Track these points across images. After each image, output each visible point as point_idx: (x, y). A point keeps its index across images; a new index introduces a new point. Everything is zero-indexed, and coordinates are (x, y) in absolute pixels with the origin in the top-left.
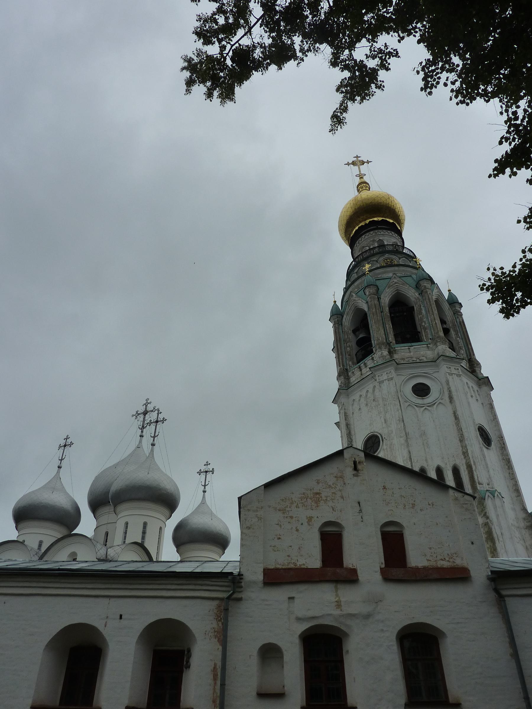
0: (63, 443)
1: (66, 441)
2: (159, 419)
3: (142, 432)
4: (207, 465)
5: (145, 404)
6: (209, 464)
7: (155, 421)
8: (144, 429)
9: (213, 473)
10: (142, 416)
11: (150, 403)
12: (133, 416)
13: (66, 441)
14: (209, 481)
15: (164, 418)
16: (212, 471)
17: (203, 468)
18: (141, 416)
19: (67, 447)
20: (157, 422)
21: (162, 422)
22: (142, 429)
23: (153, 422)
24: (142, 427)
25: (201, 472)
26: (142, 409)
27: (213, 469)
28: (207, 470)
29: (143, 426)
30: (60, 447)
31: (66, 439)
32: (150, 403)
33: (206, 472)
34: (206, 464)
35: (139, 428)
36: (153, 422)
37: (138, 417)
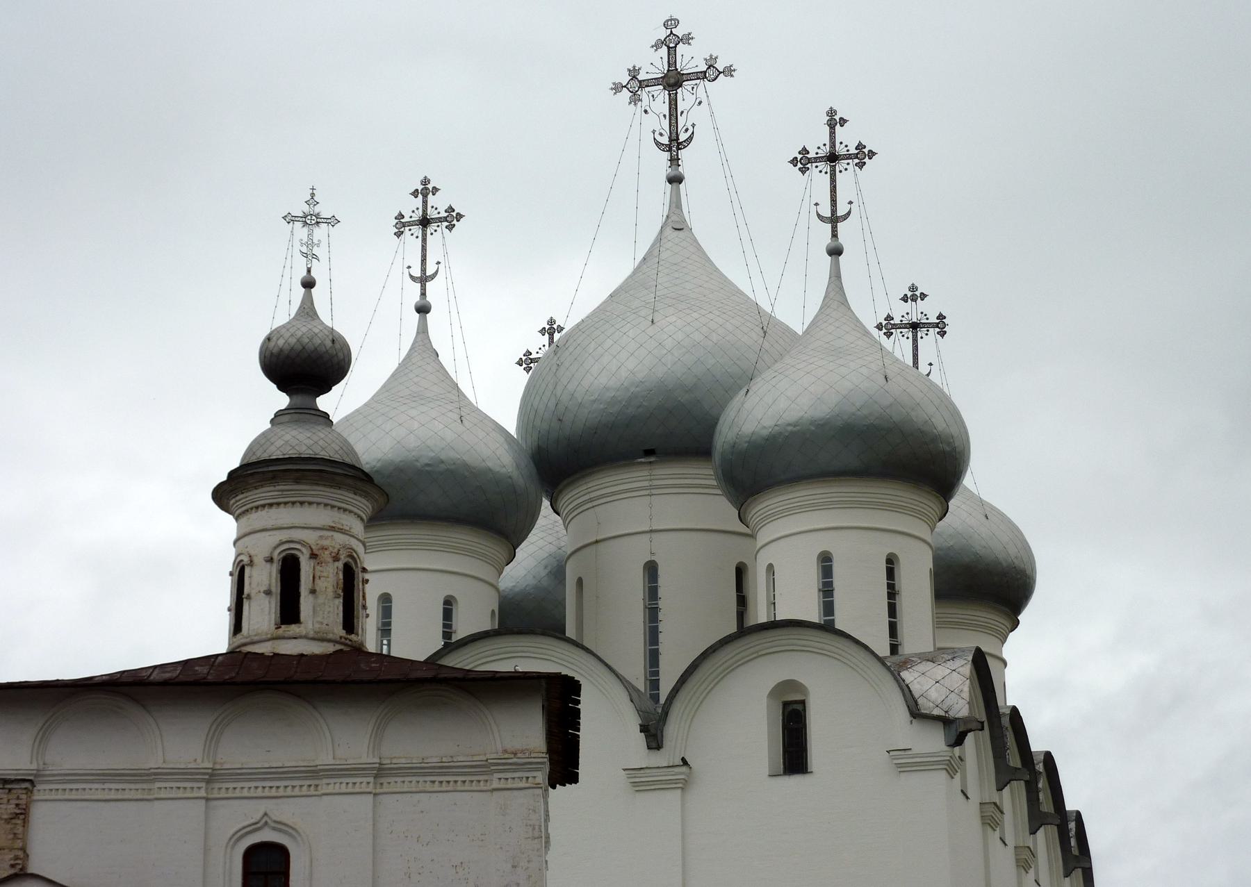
0: (412, 207)
1: (425, 203)
2: (841, 150)
3: (674, 161)
4: (914, 299)
5: (663, 42)
6: (923, 296)
7: (822, 153)
8: (679, 149)
9: (942, 334)
10: (658, 100)
11: (687, 39)
12: (617, 88)
13: (425, 203)
14: (931, 364)
15: (860, 147)
16: (936, 325)
17: (901, 312)
18: (656, 94)
19: (433, 226)
20: (833, 158)
21: (857, 161)
22: (670, 150)
23: (817, 160)
24: (671, 140)
25: (895, 326)
26: (655, 64)
27: (941, 317)
28: (915, 320)
29: (674, 135)
30: (401, 224)
31: (425, 196)
32: (687, 39)
33: (915, 326)
34: (909, 294)
35: (658, 144)
36: (817, 160)
37: (644, 94)
